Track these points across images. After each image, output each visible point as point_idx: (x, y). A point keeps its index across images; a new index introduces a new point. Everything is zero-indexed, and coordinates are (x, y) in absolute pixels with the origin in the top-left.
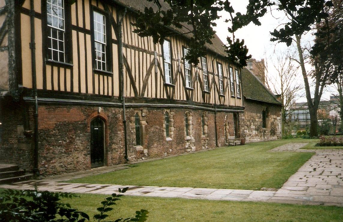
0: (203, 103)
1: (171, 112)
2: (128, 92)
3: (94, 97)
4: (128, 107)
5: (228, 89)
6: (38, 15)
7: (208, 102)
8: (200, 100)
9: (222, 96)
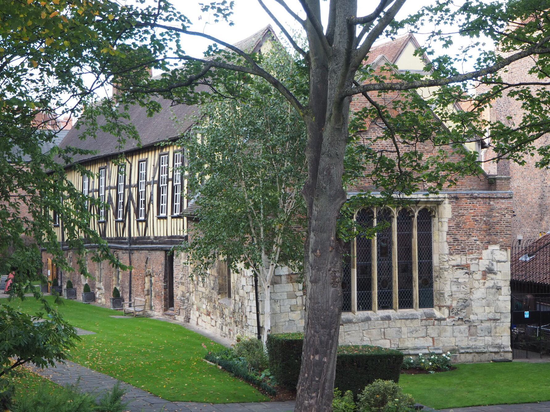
0: (116, 239)
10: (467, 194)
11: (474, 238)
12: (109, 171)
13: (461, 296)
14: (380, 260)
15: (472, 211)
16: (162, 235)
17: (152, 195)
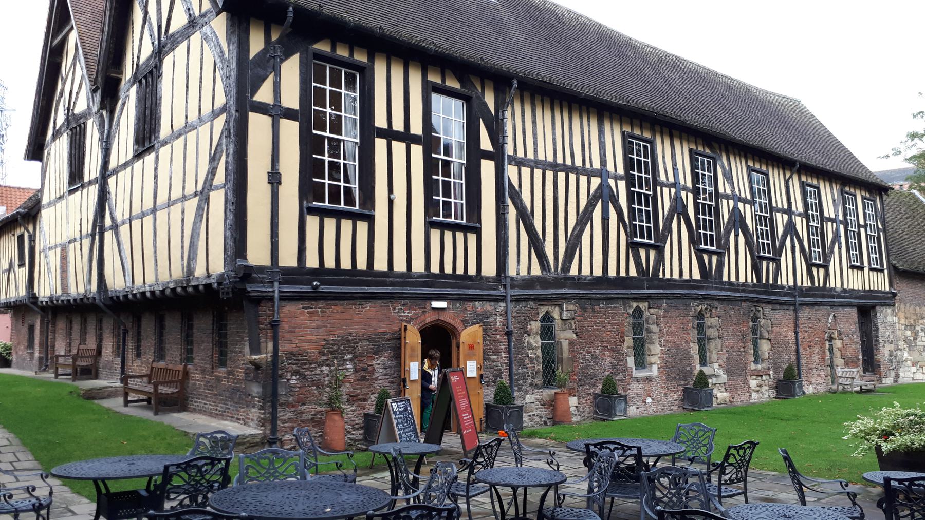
1: (649, 308)
2: (522, 265)
3: (428, 279)
4: (517, 300)
5: (840, 248)
6: (289, 114)
7: (771, 282)
8: (746, 275)
9: (818, 266)
12: (723, 167)
16: (856, 288)
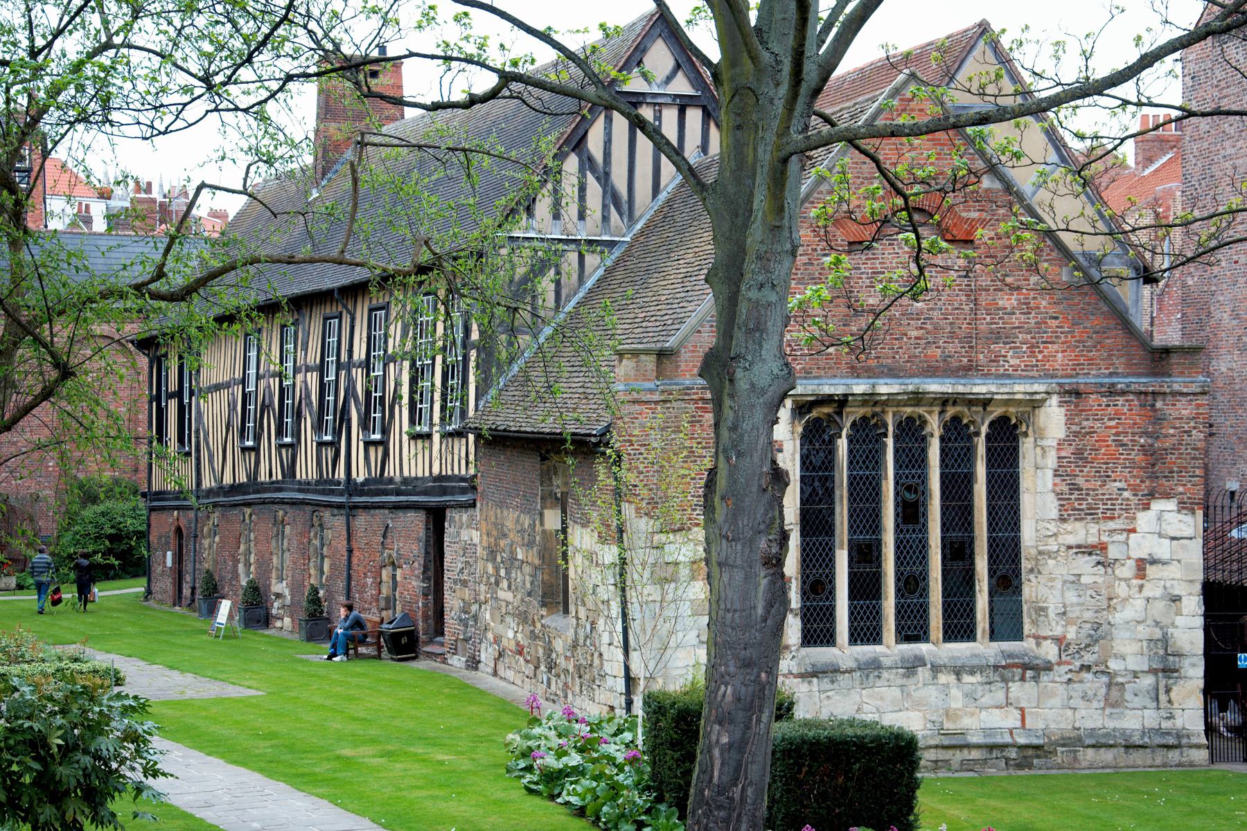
0: (318, 483)
10: (1102, 385)
11: (1118, 484)
12: (304, 329)
13: (1088, 615)
14: (902, 531)
15: (1113, 423)
16: (420, 475)
17: (398, 384)
